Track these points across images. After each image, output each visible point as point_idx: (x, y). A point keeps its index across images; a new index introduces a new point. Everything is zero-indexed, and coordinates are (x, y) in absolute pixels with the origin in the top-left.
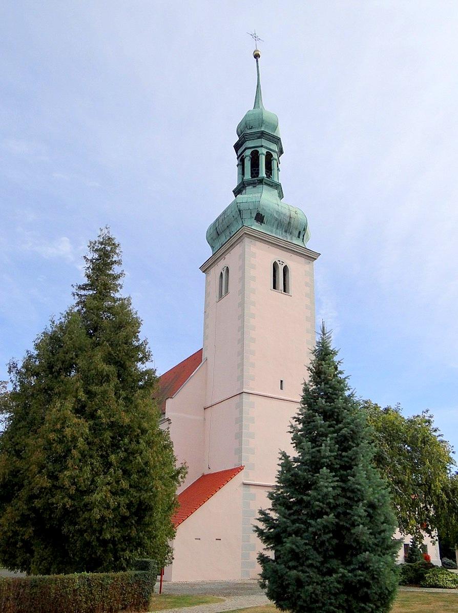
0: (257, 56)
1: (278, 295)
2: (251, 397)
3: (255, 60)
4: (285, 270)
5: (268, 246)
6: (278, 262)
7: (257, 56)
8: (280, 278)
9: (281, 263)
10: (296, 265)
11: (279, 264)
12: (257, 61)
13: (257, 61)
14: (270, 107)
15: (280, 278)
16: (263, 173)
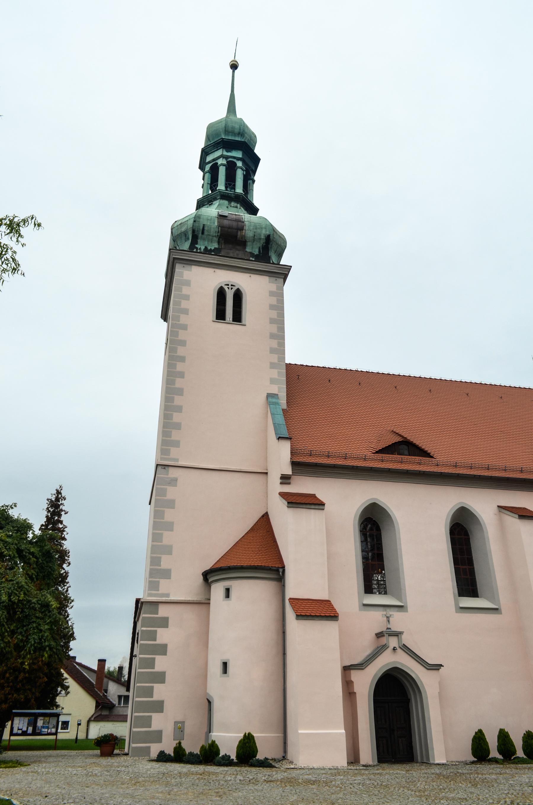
0: (234, 66)
1: (227, 328)
2: (171, 470)
3: (231, 71)
4: (238, 296)
5: (247, 275)
6: (226, 288)
7: (234, 66)
8: (229, 307)
9: (230, 287)
10: (253, 286)
11: (227, 289)
12: (234, 72)
13: (234, 72)
14: (249, 115)
15: (229, 307)
16: (221, 186)
